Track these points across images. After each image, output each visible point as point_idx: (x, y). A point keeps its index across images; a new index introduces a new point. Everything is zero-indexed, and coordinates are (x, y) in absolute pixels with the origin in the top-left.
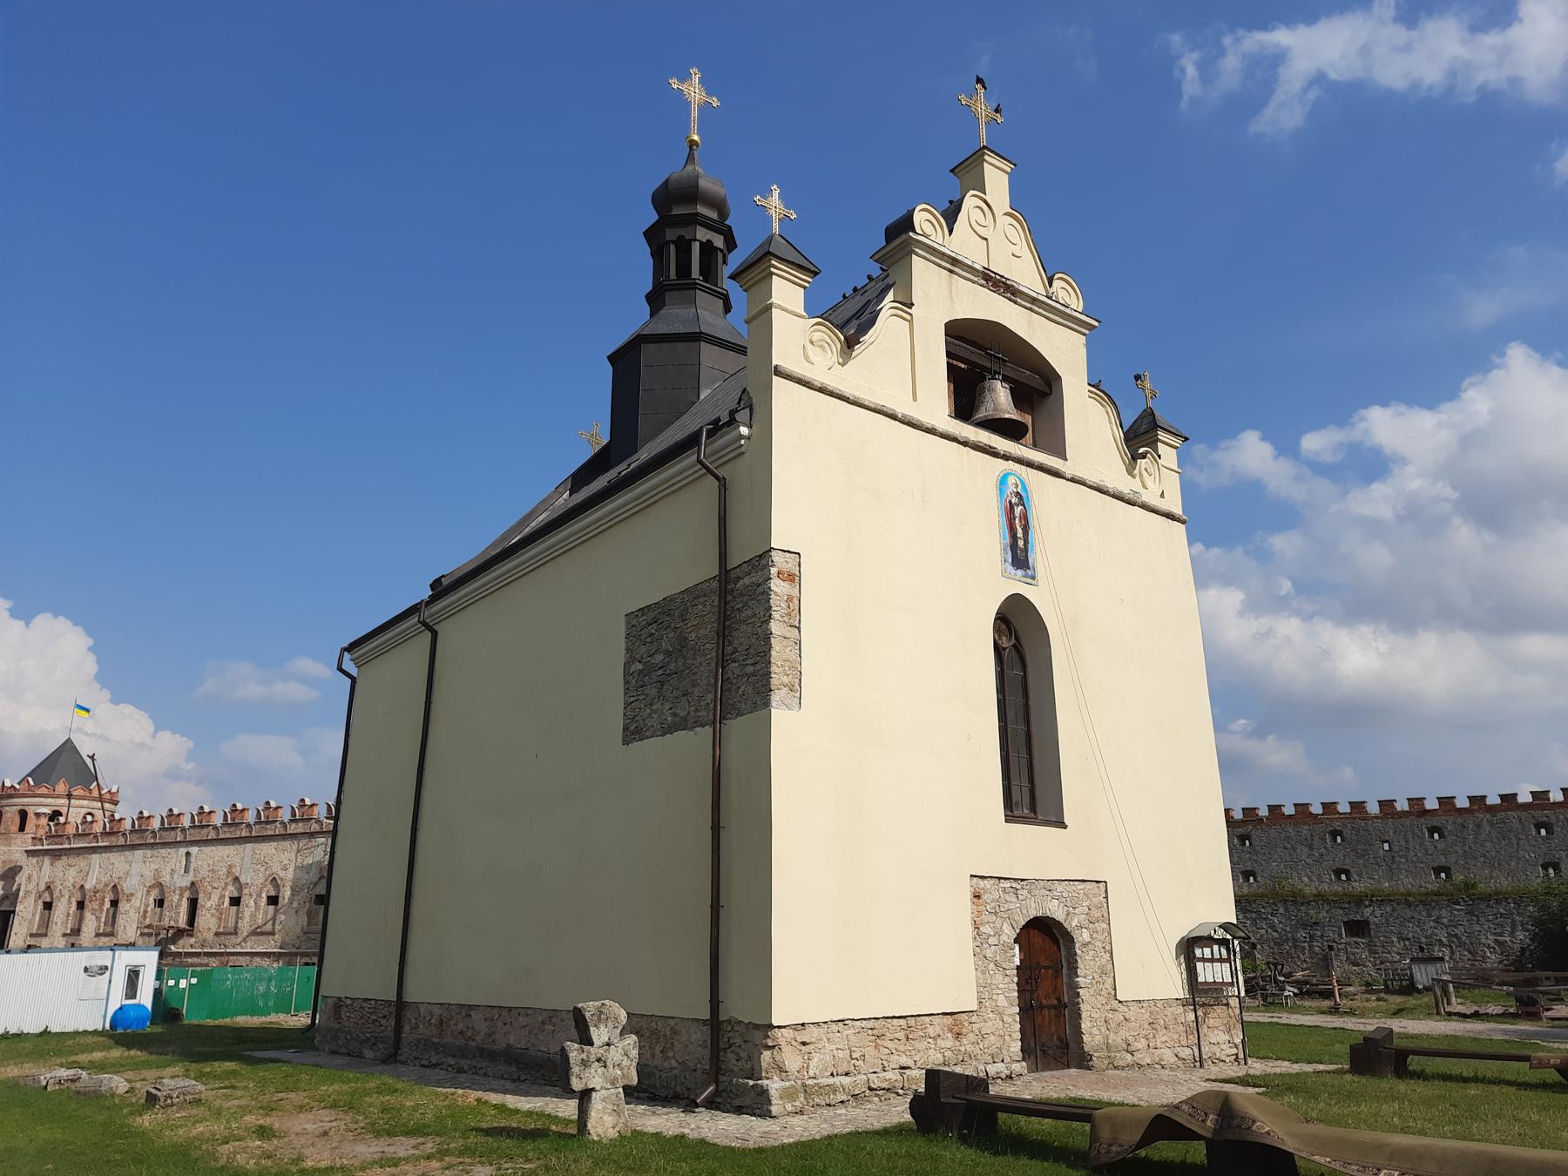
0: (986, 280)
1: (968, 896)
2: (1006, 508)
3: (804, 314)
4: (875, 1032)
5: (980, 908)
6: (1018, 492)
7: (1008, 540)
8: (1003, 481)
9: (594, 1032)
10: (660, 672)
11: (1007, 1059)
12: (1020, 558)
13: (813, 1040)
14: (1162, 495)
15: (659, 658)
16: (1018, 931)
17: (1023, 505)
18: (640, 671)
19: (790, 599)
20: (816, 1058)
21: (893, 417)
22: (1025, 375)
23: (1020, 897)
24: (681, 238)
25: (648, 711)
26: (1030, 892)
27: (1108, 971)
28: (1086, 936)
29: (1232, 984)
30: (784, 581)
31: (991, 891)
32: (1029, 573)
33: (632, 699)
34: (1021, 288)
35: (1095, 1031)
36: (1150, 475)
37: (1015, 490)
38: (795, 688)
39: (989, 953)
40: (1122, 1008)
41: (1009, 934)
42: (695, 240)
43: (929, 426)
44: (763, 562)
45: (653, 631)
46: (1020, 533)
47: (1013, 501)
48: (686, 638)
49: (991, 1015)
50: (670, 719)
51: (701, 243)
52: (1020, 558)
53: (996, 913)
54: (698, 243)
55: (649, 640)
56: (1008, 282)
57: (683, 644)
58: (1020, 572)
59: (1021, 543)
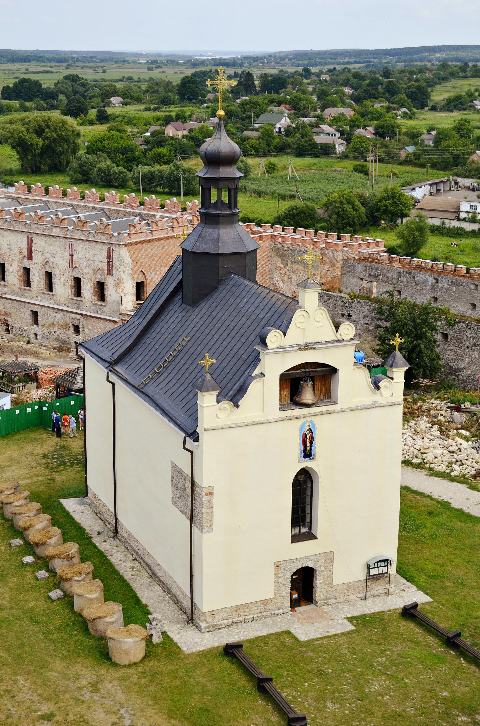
1: (273, 566)
2: (303, 437)
8: (302, 428)
9: (152, 623)
11: (284, 608)
12: (307, 454)
17: (313, 433)
19: (210, 500)
20: (217, 617)
27: (330, 577)
28: (322, 568)
29: (387, 573)
32: (311, 458)
35: (322, 595)
38: (211, 526)
41: (289, 575)
46: (308, 444)
52: (307, 454)
58: (307, 459)
59: (308, 448)
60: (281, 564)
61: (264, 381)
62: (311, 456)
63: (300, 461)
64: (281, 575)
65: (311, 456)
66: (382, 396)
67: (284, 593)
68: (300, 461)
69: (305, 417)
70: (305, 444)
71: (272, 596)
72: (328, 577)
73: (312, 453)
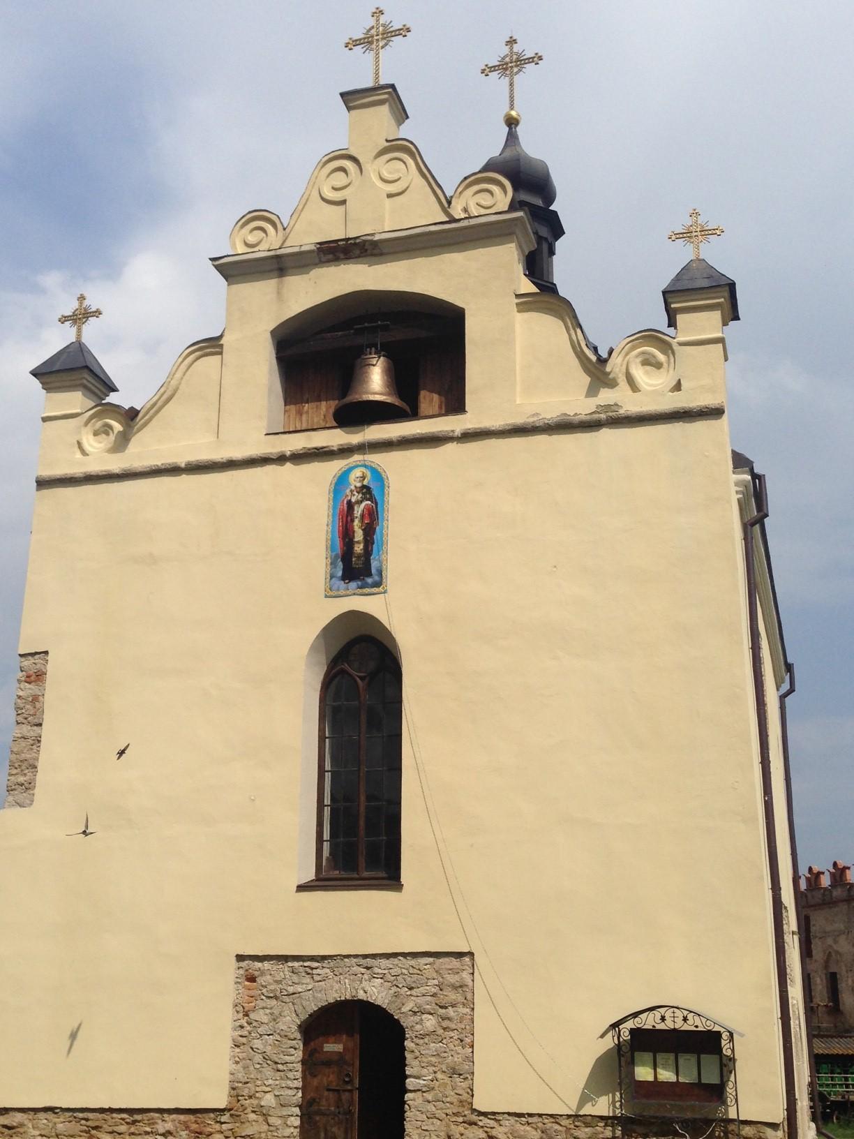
0: (333, 253)
2: (341, 512)
4: (89, 1123)
5: (252, 993)
6: (364, 487)
13: (15, 1124)
14: (678, 387)
16: (304, 1016)
21: (174, 470)
27: (462, 1073)
28: (430, 1023)
30: (30, 683)
31: (271, 974)
32: (369, 580)
34: (377, 238)
36: (658, 366)
37: (359, 485)
39: (257, 1044)
40: (485, 1121)
41: (290, 1022)
43: (224, 460)
46: (359, 535)
47: (353, 500)
49: (252, 1116)
53: (276, 998)
56: (358, 241)
58: (353, 585)
59: (359, 548)
60: (263, 973)
61: (221, 353)
62: (370, 575)
63: (331, 594)
64: (260, 1016)
65: (370, 575)
66: (633, 386)
67: (269, 1100)
68: (331, 594)
69: (346, 451)
70: (346, 535)
71: (220, 1100)
72: (454, 1072)
73: (374, 565)
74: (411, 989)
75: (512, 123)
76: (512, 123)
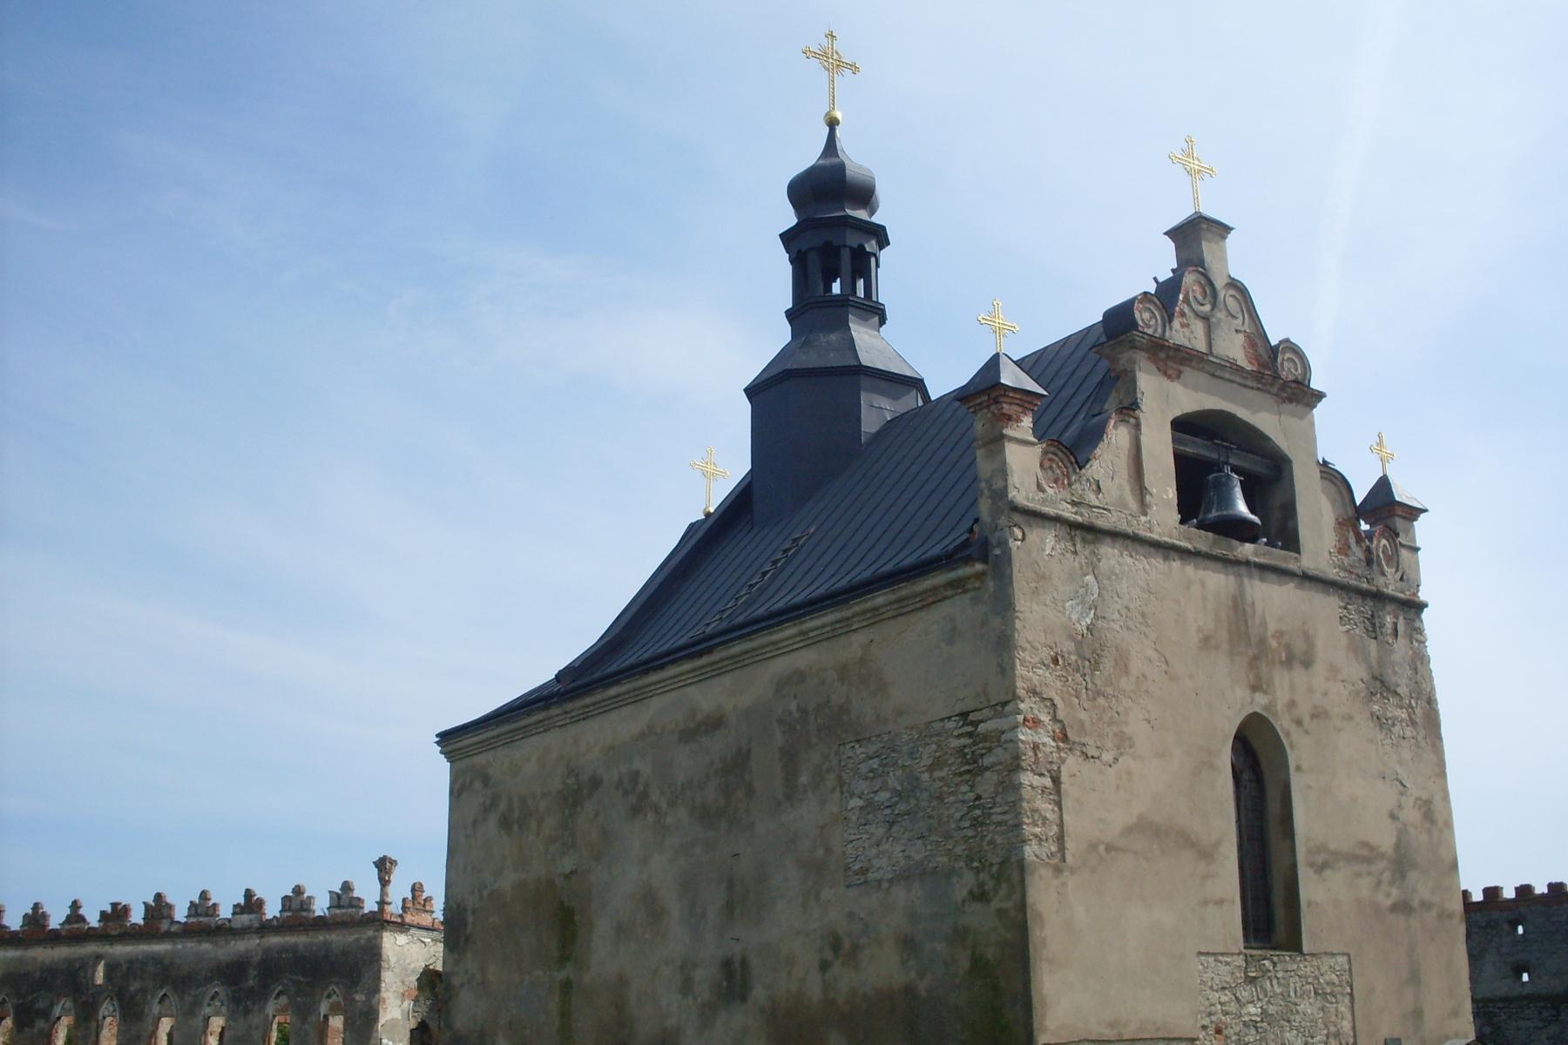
3: (1032, 439)
7: (1219, 565)
10: (888, 811)
15: (884, 796)
18: (862, 808)
22: (1256, 465)
23: (1260, 1030)
24: (827, 244)
25: (874, 851)
26: (1269, 1024)
33: (853, 837)
42: (845, 246)
44: (1008, 708)
45: (875, 766)
48: (917, 779)
50: (902, 862)
51: (851, 248)
54: (848, 249)
55: (871, 775)
57: (915, 784)
74: (1312, 1038)
75: (832, 124)
76: (832, 124)
